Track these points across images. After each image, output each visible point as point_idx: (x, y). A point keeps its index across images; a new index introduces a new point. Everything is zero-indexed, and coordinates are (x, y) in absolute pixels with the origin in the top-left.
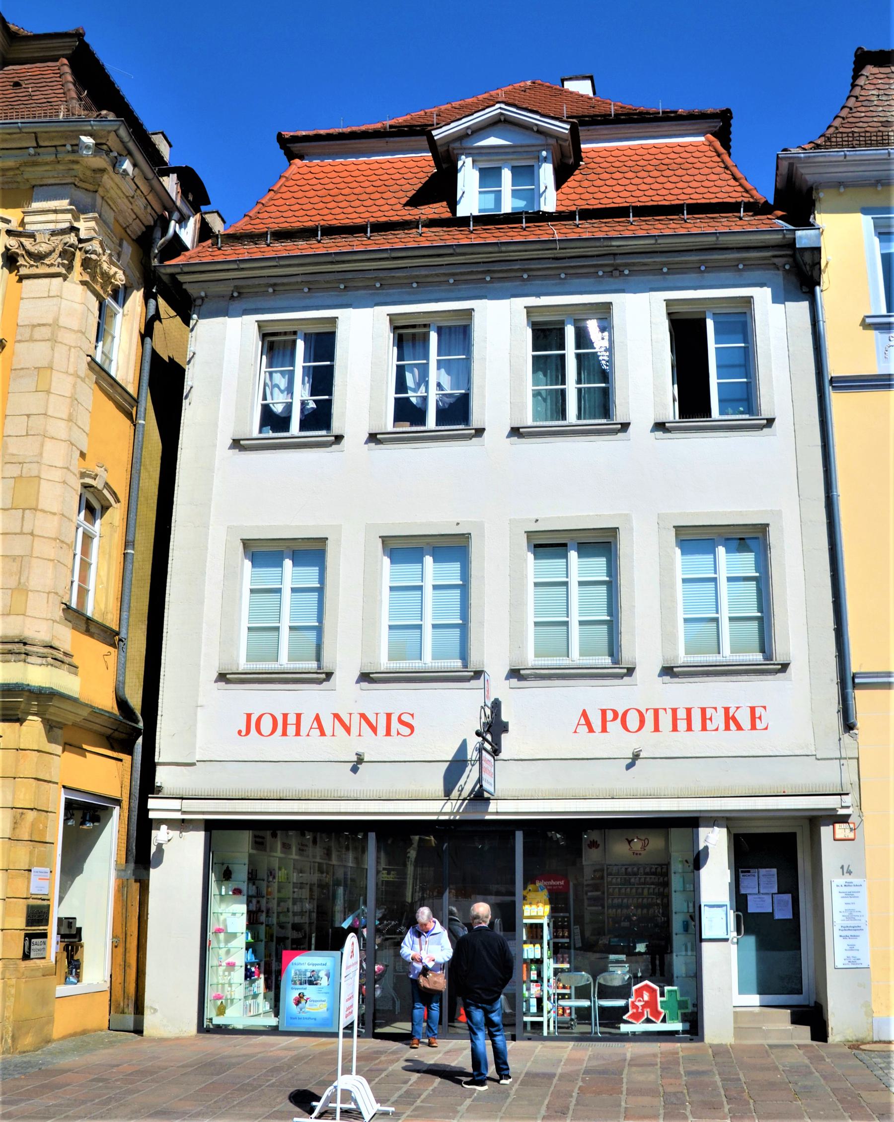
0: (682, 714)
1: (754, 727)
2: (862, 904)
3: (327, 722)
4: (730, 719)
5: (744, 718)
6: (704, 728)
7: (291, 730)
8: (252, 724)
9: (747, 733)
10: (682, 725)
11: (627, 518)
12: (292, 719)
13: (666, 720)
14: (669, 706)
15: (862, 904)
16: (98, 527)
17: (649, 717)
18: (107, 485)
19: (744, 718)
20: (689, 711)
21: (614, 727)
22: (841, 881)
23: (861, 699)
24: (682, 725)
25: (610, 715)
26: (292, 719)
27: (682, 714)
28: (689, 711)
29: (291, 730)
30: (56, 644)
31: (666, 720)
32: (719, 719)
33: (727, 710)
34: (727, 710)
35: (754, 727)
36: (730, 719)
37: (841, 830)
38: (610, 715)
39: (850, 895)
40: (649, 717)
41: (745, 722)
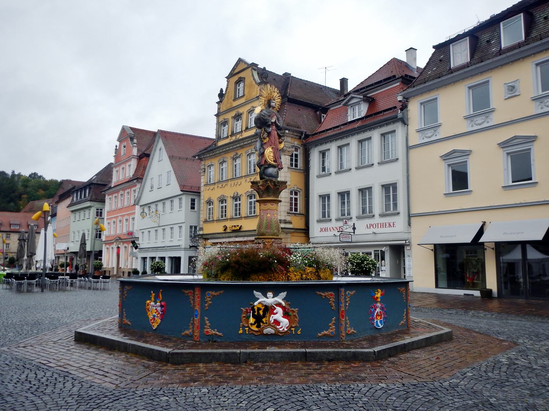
0: (382, 224)
1: (393, 227)
2: (411, 263)
3: (331, 228)
4: (390, 225)
5: (392, 225)
6: (385, 227)
7: (327, 230)
8: (321, 230)
9: (392, 228)
10: (382, 226)
11: (373, 184)
12: (327, 229)
13: (379, 225)
14: (380, 223)
15: (411, 263)
16: (298, 197)
17: (377, 225)
18: (297, 188)
19: (392, 225)
20: (383, 223)
21: (372, 227)
22: (408, 258)
23: (413, 219)
24: (382, 226)
25: (371, 225)
26: (327, 229)
27: (382, 224)
28: (383, 223)
29: (327, 230)
30: (286, 220)
31: (379, 225)
32: (388, 225)
33: (389, 223)
34: (389, 223)
35: (393, 227)
36: (390, 225)
37: (408, 248)
38: (371, 225)
39: (409, 261)
40: (377, 225)
41: (392, 225)
